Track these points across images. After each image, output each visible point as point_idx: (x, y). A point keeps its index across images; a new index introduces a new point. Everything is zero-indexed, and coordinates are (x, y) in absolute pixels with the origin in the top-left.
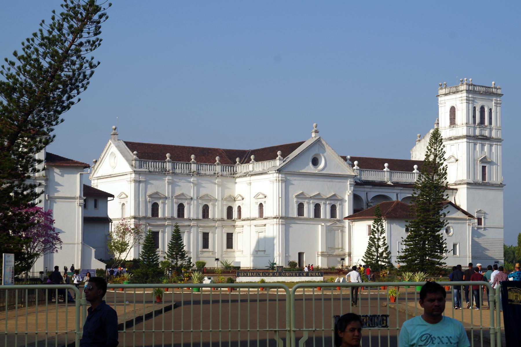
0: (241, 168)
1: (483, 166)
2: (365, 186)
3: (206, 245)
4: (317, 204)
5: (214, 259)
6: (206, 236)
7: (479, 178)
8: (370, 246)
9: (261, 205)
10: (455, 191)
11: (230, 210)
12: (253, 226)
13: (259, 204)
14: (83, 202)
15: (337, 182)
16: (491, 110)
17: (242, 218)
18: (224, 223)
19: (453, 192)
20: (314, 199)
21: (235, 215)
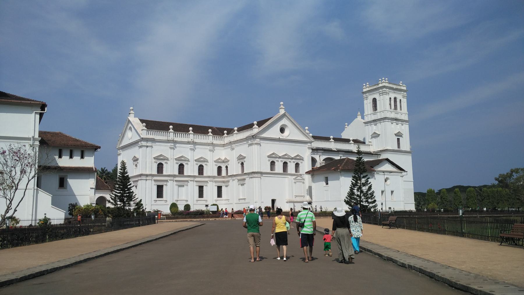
0: (227, 139)
1: (398, 138)
2: (319, 151)
3: (201, 195)
4: (285, 162)
5: (205, 205)
6: (201, 188)
7: (396, 148)
8: (354, 185)
9: (242, 164)
10: (379, 156)
11: (219, 169)
13: (240, 163)
14: (38, 144)
15: (300, 146)
16: (400, 100)
17: (228, 175)
19: (378, 157)
21: (224, 173)
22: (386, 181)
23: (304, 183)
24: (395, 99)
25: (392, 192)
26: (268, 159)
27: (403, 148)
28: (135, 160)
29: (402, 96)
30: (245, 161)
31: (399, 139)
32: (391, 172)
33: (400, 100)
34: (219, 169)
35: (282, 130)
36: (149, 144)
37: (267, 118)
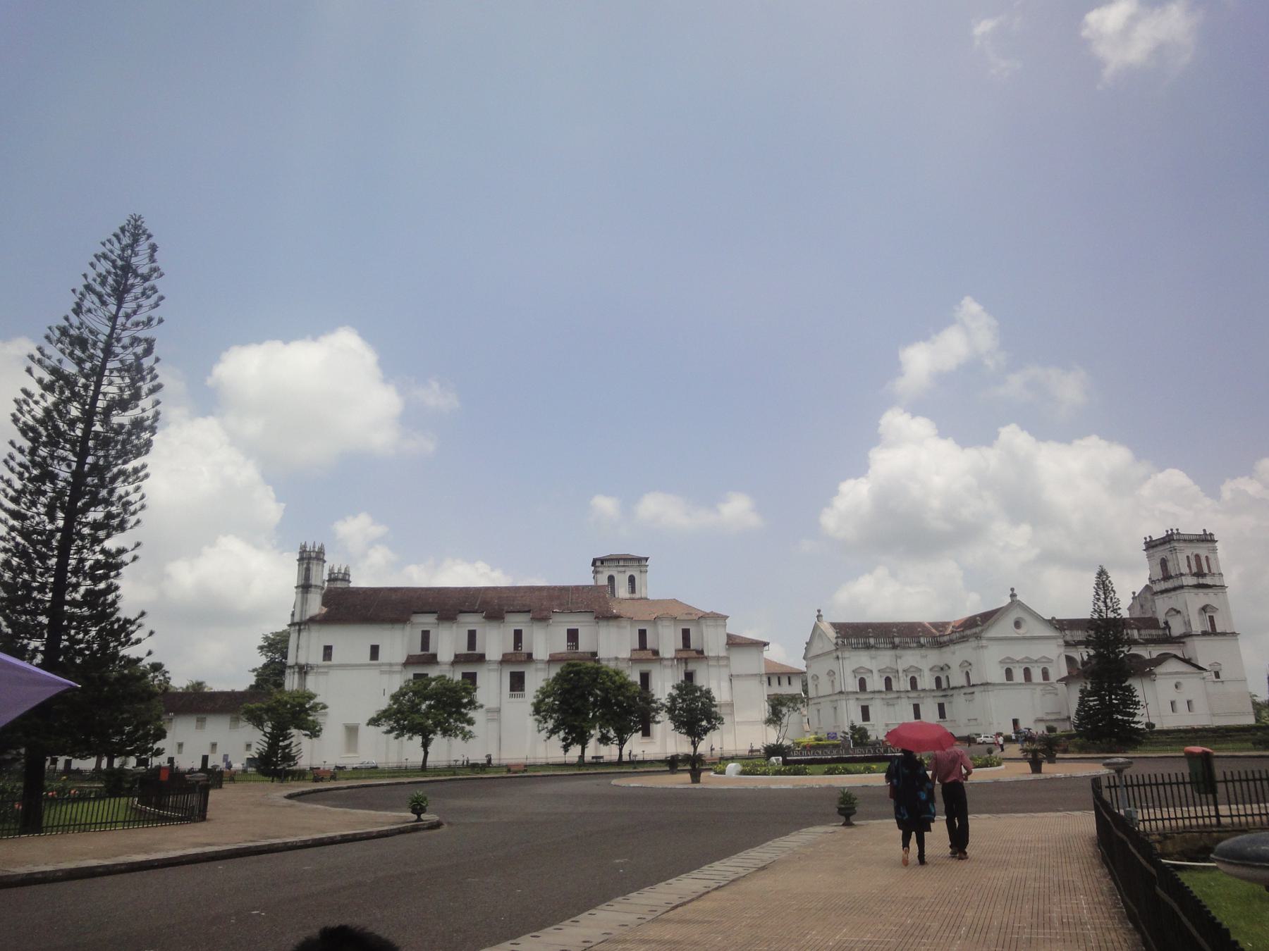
1: (1209, 616)
6: (916, 708)
9: (967, 674)
10: (1182, 645)
12: (962, 695)
16: (1207, 557)
18: (933, 694)
20: (1022, 663)
21: (944, 685)
22: (1176, 687)
23: (1057, 694)
24: (1197, 557)
25: (1189, 702)
26: (1002, 665)
27: (1218, 631)
28: (831, 673)
29: (1209, 550)
30: (970, 670)
31: (1212, 617)
32: (1186, 673)
33: (1207, 557)
34: (938, 680)
35: (1017, 624)
36: (847, 654)
37: (994, 608)
